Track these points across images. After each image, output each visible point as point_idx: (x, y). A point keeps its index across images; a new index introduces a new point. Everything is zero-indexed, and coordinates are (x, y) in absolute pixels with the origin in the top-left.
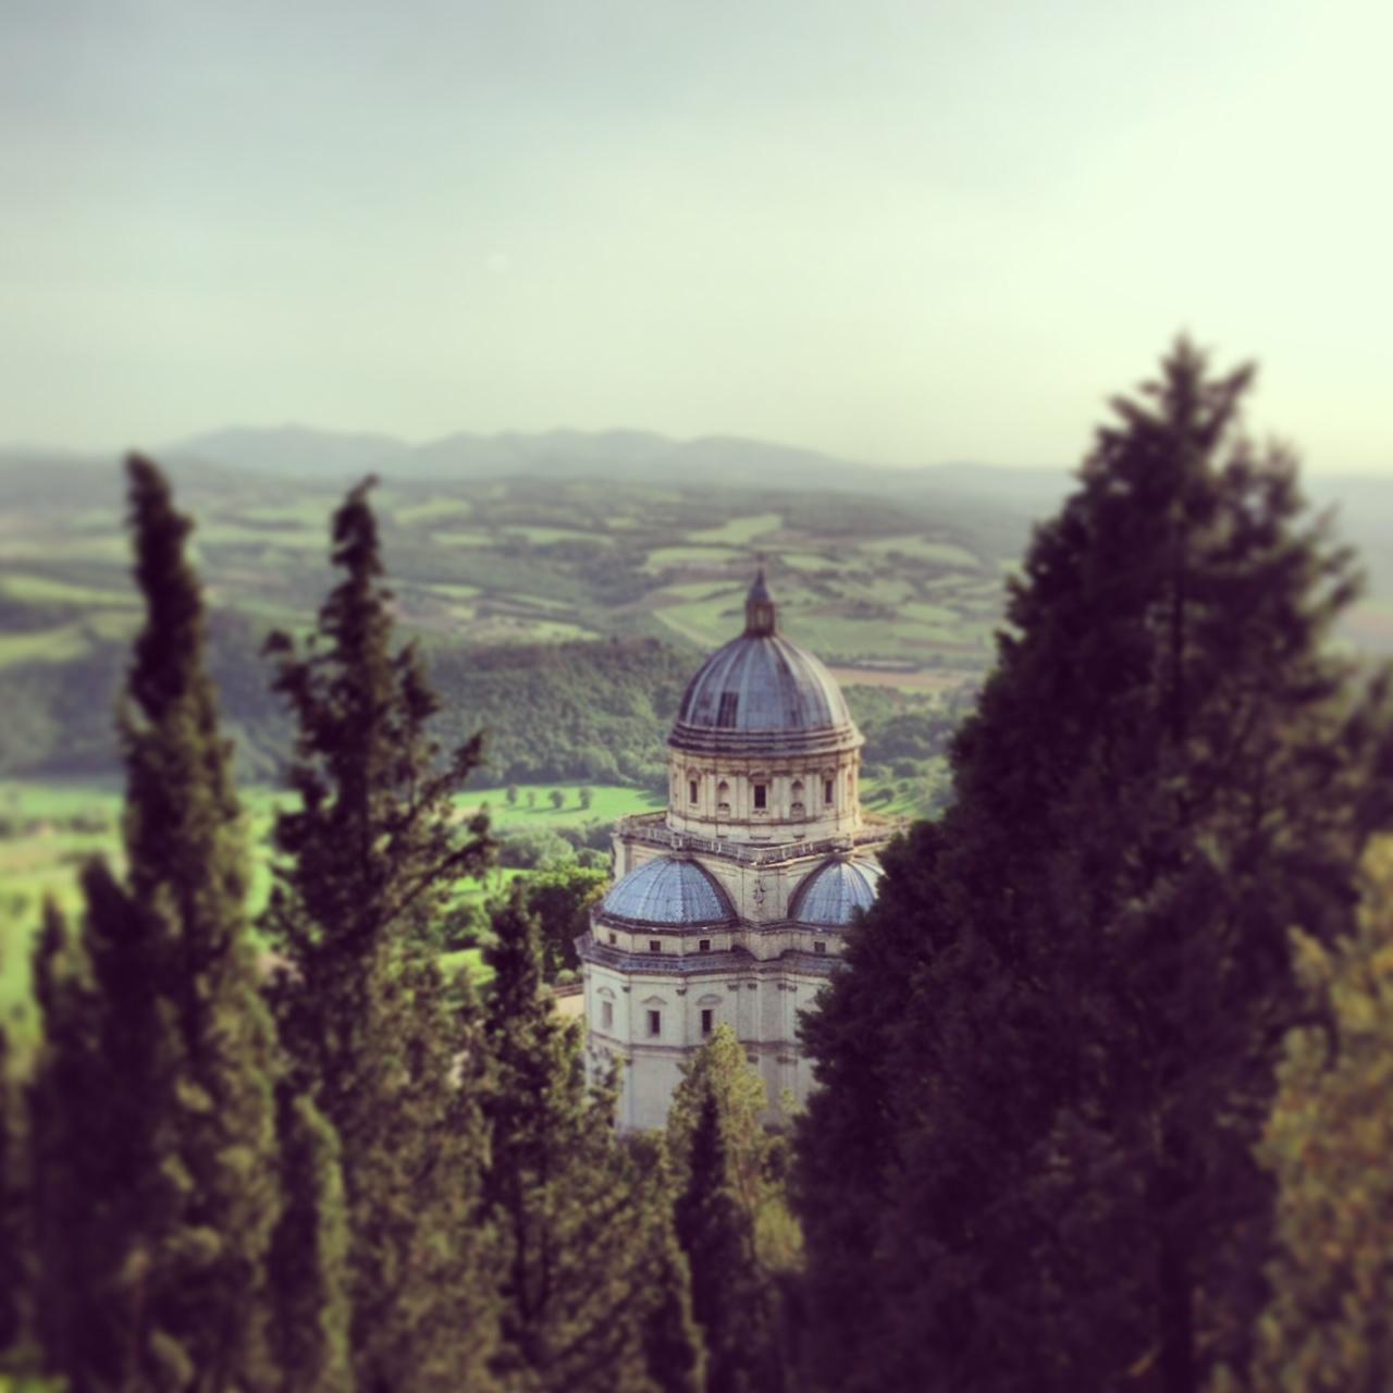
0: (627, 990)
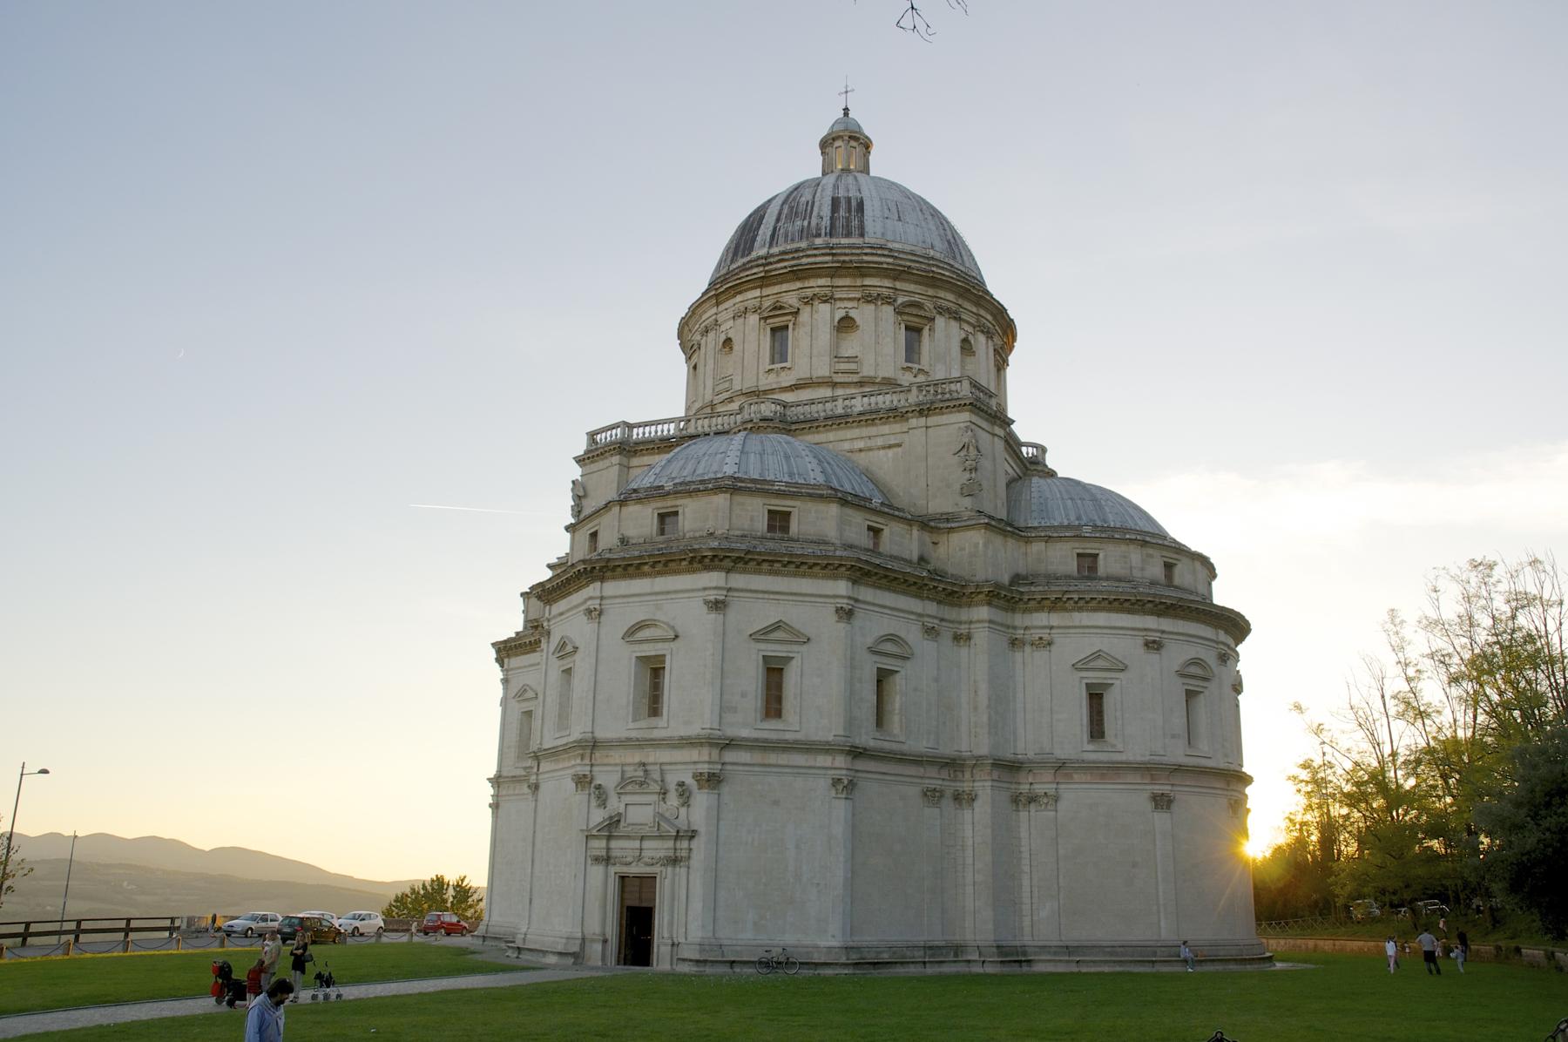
0: (718, 606)
